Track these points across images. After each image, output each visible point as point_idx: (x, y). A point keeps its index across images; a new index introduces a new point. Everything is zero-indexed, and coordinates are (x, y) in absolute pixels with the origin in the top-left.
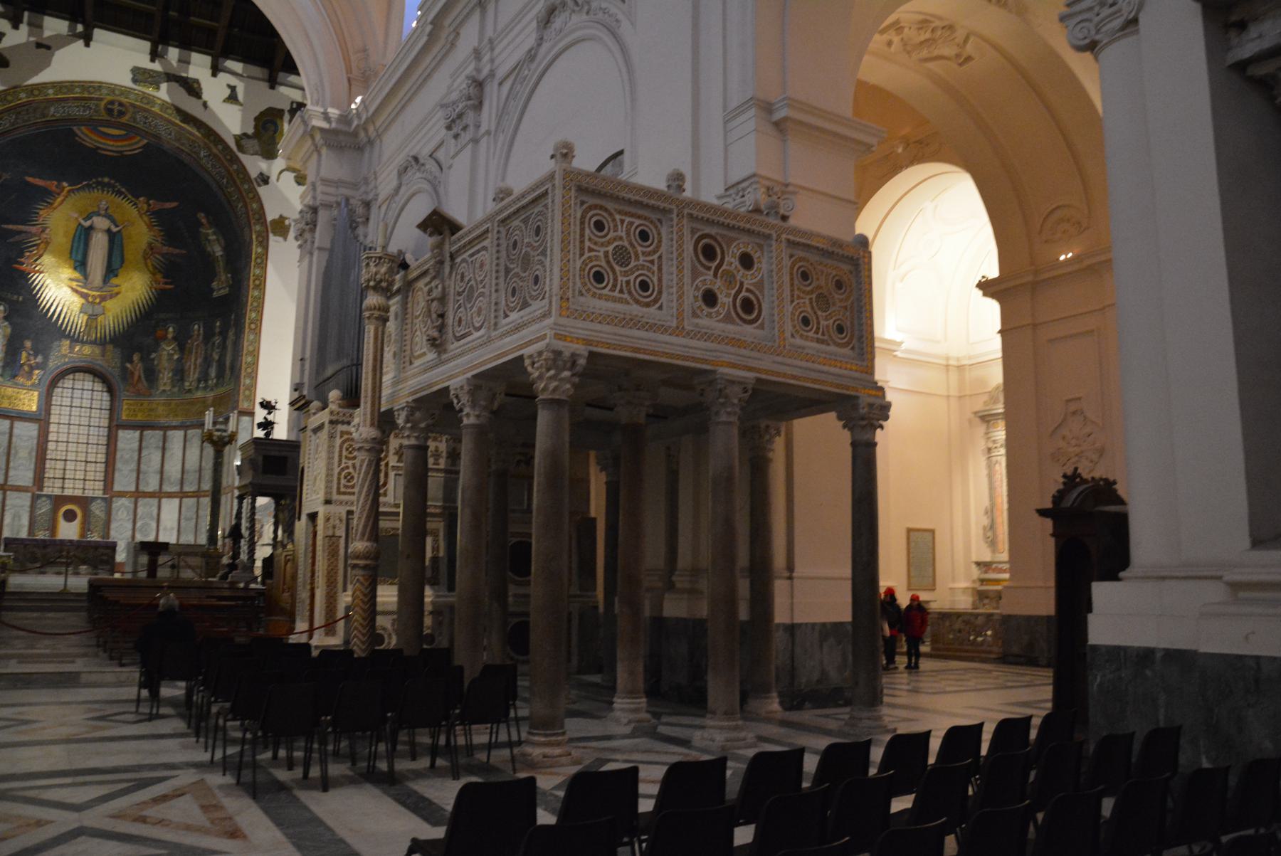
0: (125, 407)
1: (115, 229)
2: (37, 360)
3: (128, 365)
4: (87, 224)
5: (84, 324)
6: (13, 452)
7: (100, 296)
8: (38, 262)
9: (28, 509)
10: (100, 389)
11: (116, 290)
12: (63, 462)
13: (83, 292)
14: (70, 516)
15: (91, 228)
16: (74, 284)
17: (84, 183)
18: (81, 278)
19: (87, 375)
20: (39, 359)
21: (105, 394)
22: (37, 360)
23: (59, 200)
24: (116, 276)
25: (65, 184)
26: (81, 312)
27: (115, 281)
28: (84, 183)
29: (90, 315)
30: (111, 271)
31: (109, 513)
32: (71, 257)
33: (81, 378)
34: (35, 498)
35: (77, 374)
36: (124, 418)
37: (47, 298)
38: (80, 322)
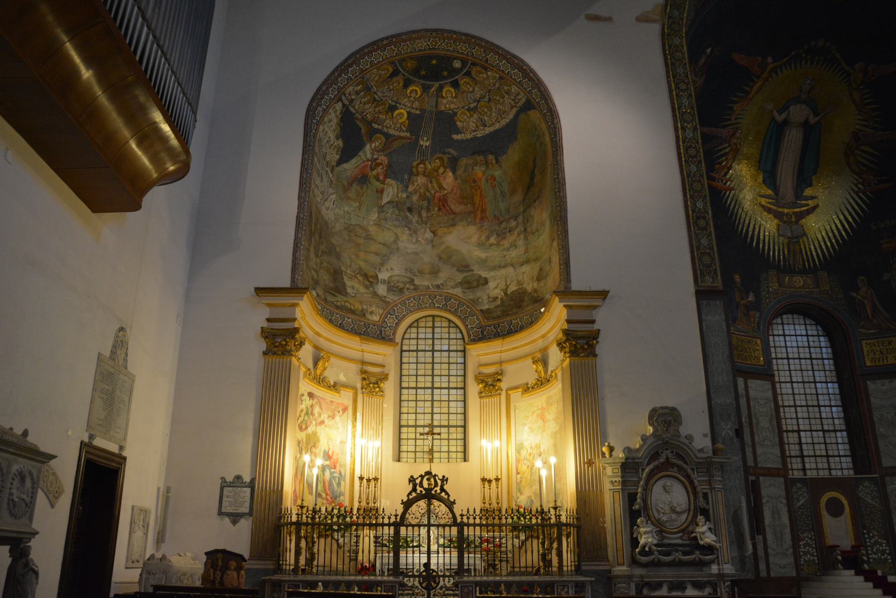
0: (865, 350)
1: (813, 120)
2: (750, 299)
3: (855, 295)
4: (780, 118)
5: (786, 250)
6: (754, 421)
7: (794, 213)
8: (728, 177)
9: (785, 501)
10: (815, 333)
11: (811, 203)
12: (796, 435)
13: (775, 211)
14: (835, 509)
15: (786, 122)
16: (763, 201)
17: (793, 54)
18: (773, 194)
19: (795, 316)
20: (751, 298)
21: (822, 339)
22: (750, 299)
23: (758, 85)
24: (811, 185)
25: (770, 60)
26: (779, 235)
27: (808, 192)
28: (793, 54)
29: (789, 238)
30: (803, 179)
31: (884, 498)
32: (759, 169)
33: (791, 321)
34: (790, 484)
35: (785, 316)
36: (868, 363)
37: (742, 221)
38: (776, 248)
